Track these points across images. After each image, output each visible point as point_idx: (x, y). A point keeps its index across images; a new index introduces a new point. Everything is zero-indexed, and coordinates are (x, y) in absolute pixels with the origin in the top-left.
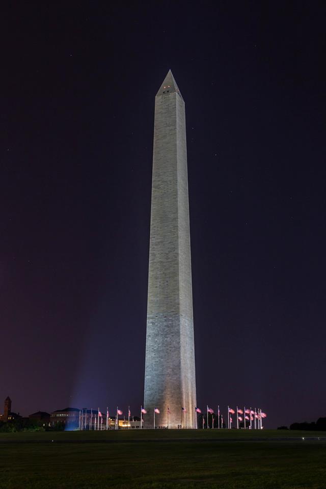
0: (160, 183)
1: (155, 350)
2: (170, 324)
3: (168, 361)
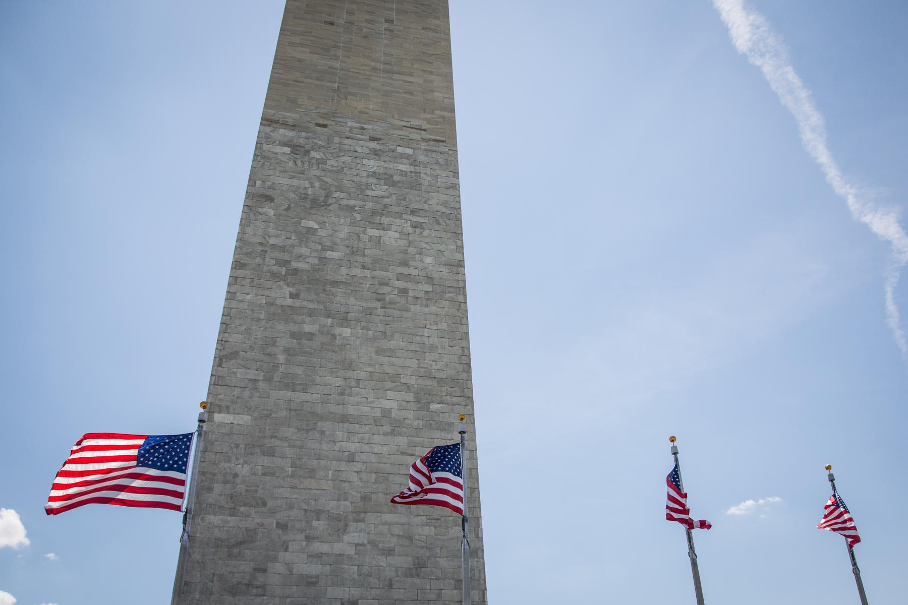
1: (296, 271)
2: (403, 173)
3: (384, 344)
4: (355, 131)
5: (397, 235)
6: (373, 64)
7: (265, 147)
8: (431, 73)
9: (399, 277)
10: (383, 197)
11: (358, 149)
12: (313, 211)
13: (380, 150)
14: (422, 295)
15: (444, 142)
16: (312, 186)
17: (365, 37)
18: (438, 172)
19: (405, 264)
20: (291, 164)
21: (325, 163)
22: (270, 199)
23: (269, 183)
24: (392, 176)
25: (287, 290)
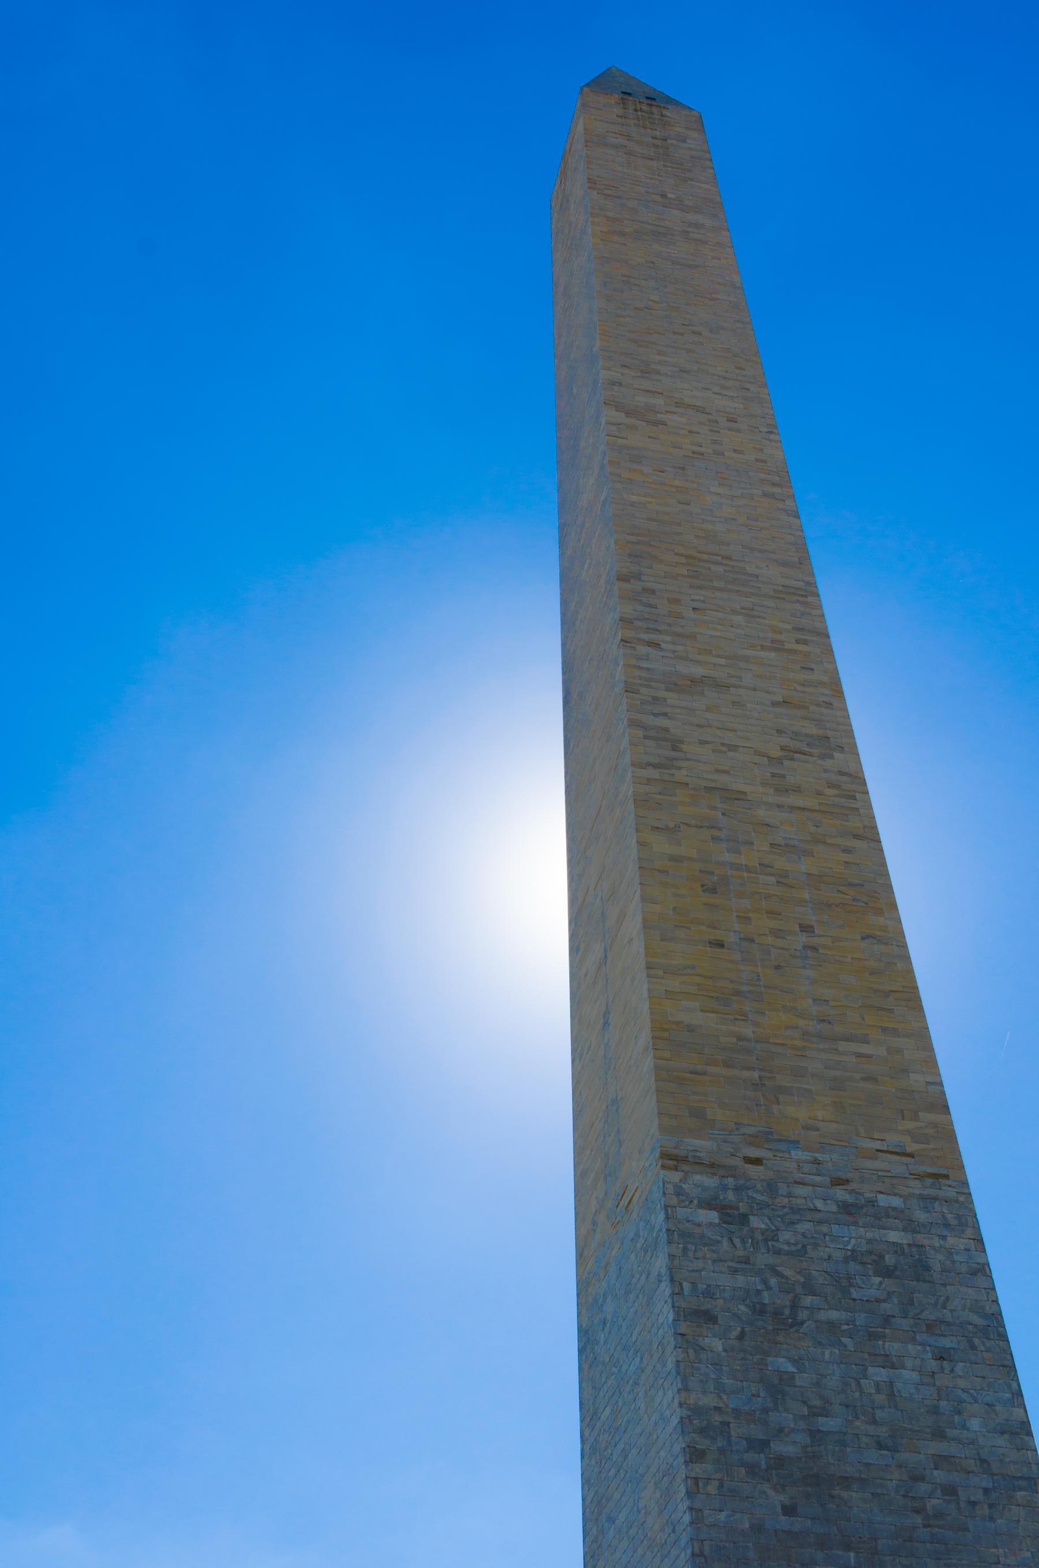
1: (781, 1461)
2: (897, 1249)
4: (806, 1167)
5: (915, 1376)
6: (801, 1022)
7: (681, 1212)
8: (895, 1032)
9: (940, 1461)
10: (878, 1301)
11: (819, 1204)
12: (780, 1338)
13: (852, 1205)
14: (979, 1496)
15: (946, 1177)
16: (769, 1288)
17: (777, 967)
18: (951, 1241)
19: (939, 1434)
20: (725, 1243)
21: (775, 1238)
22: (710, 1318)
23: (702, 1287)
24: (881, 1257)
25: (777, 1499)
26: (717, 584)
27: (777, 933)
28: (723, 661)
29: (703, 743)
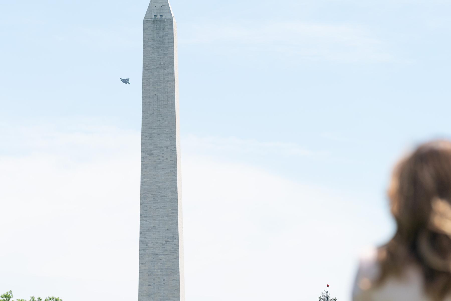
0: (152, 147)
26: (159, 201)
27: (159, 282)
28: (157, 222)
29: (152, 243)
